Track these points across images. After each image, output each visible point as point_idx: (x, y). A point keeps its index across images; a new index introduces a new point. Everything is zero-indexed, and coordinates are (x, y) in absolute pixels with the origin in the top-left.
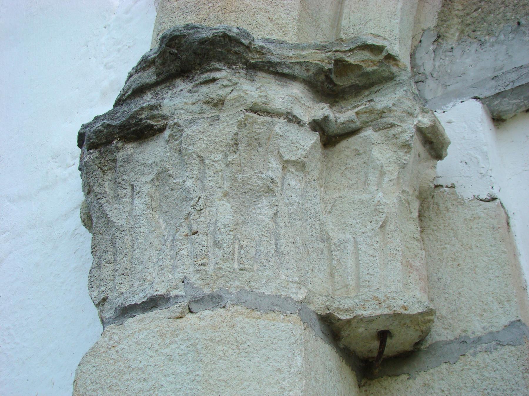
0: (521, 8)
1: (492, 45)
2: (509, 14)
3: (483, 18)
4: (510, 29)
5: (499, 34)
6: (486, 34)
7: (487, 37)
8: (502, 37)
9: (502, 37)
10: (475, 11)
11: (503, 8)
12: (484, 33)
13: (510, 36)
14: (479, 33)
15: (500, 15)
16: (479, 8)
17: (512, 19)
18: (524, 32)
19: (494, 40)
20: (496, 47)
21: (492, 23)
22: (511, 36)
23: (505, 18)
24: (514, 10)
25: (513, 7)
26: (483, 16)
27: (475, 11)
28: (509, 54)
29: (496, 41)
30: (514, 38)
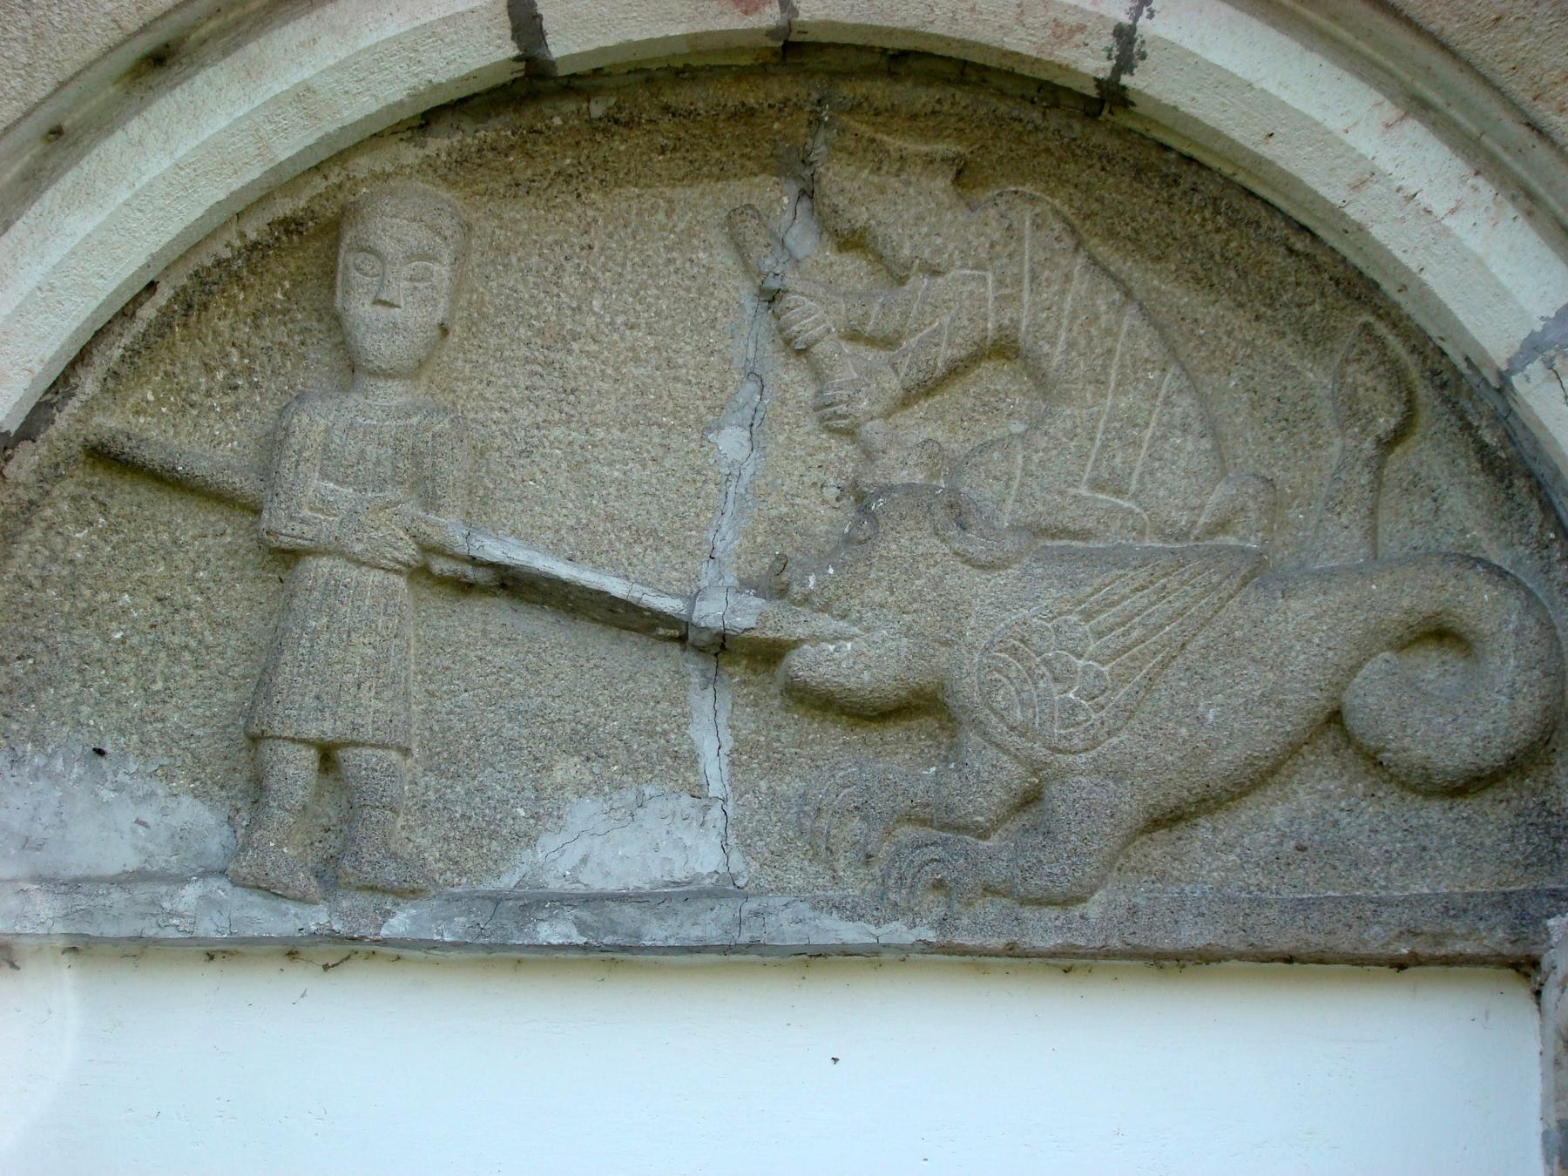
0: (113, 706)
1: (35, 777)
2: (85, 710)
3: (30, 689)
4: (79, 749)
5: (54, 752)
6: (28, 737)
7: (29, 746)
8: (59, 764)
9: (59, 764)
10: (19, 658)
11: (77, 685)
12: (25, 733)
13: (75, 770)
14: (15, 727)
15: (69, 700)
16: (29, 657)
17: (88, 725)
18: (103, 775)
19: (42, 764)
20: (42, 784)
21: (48, 714)
22: (77, 770)
23: (76, 716)
24: (97, 704)
25: (98, 695)
26: (33, 684)
27: (19, 658)
28: (63, 817)
29: (45, 766)
30: (80, 780)
